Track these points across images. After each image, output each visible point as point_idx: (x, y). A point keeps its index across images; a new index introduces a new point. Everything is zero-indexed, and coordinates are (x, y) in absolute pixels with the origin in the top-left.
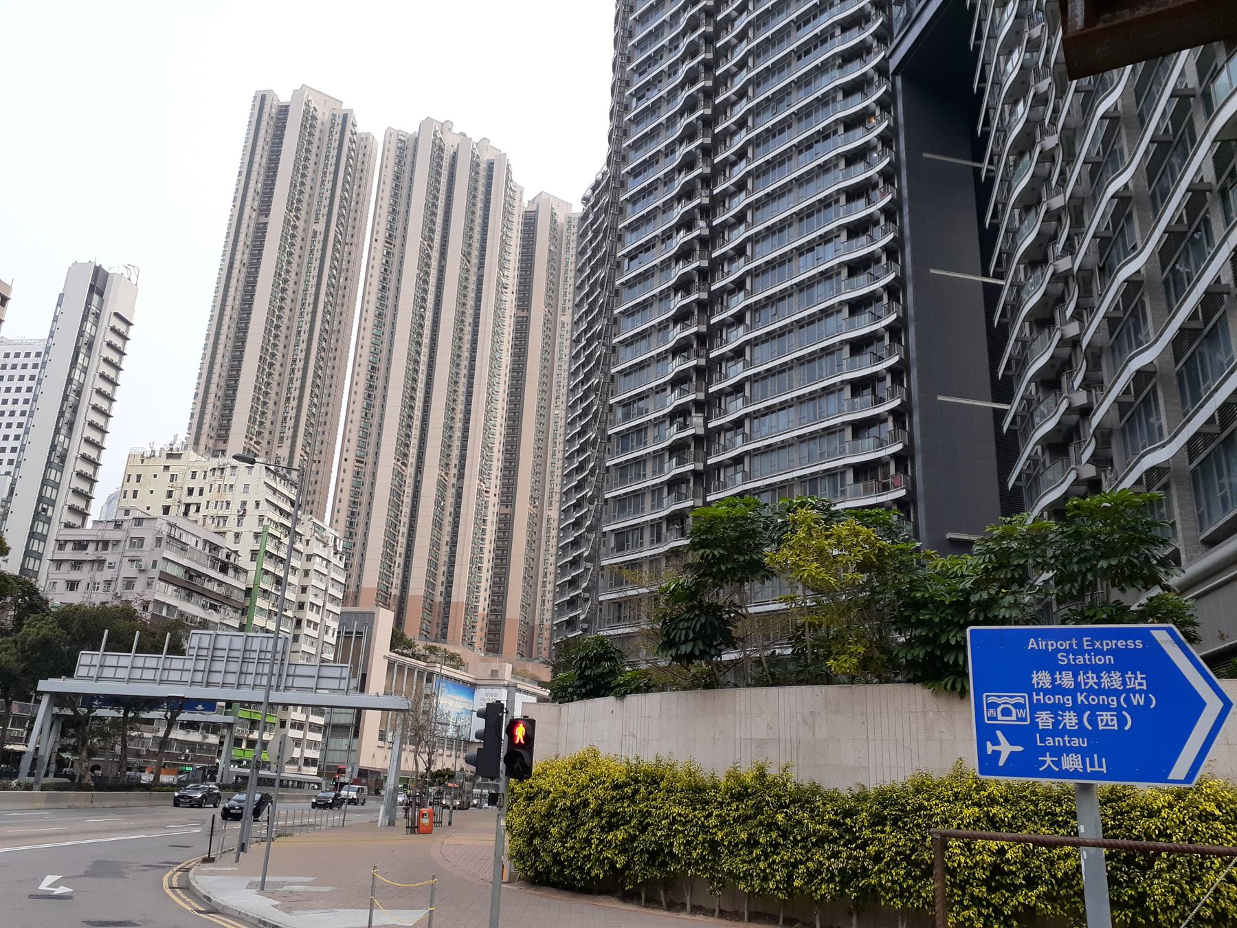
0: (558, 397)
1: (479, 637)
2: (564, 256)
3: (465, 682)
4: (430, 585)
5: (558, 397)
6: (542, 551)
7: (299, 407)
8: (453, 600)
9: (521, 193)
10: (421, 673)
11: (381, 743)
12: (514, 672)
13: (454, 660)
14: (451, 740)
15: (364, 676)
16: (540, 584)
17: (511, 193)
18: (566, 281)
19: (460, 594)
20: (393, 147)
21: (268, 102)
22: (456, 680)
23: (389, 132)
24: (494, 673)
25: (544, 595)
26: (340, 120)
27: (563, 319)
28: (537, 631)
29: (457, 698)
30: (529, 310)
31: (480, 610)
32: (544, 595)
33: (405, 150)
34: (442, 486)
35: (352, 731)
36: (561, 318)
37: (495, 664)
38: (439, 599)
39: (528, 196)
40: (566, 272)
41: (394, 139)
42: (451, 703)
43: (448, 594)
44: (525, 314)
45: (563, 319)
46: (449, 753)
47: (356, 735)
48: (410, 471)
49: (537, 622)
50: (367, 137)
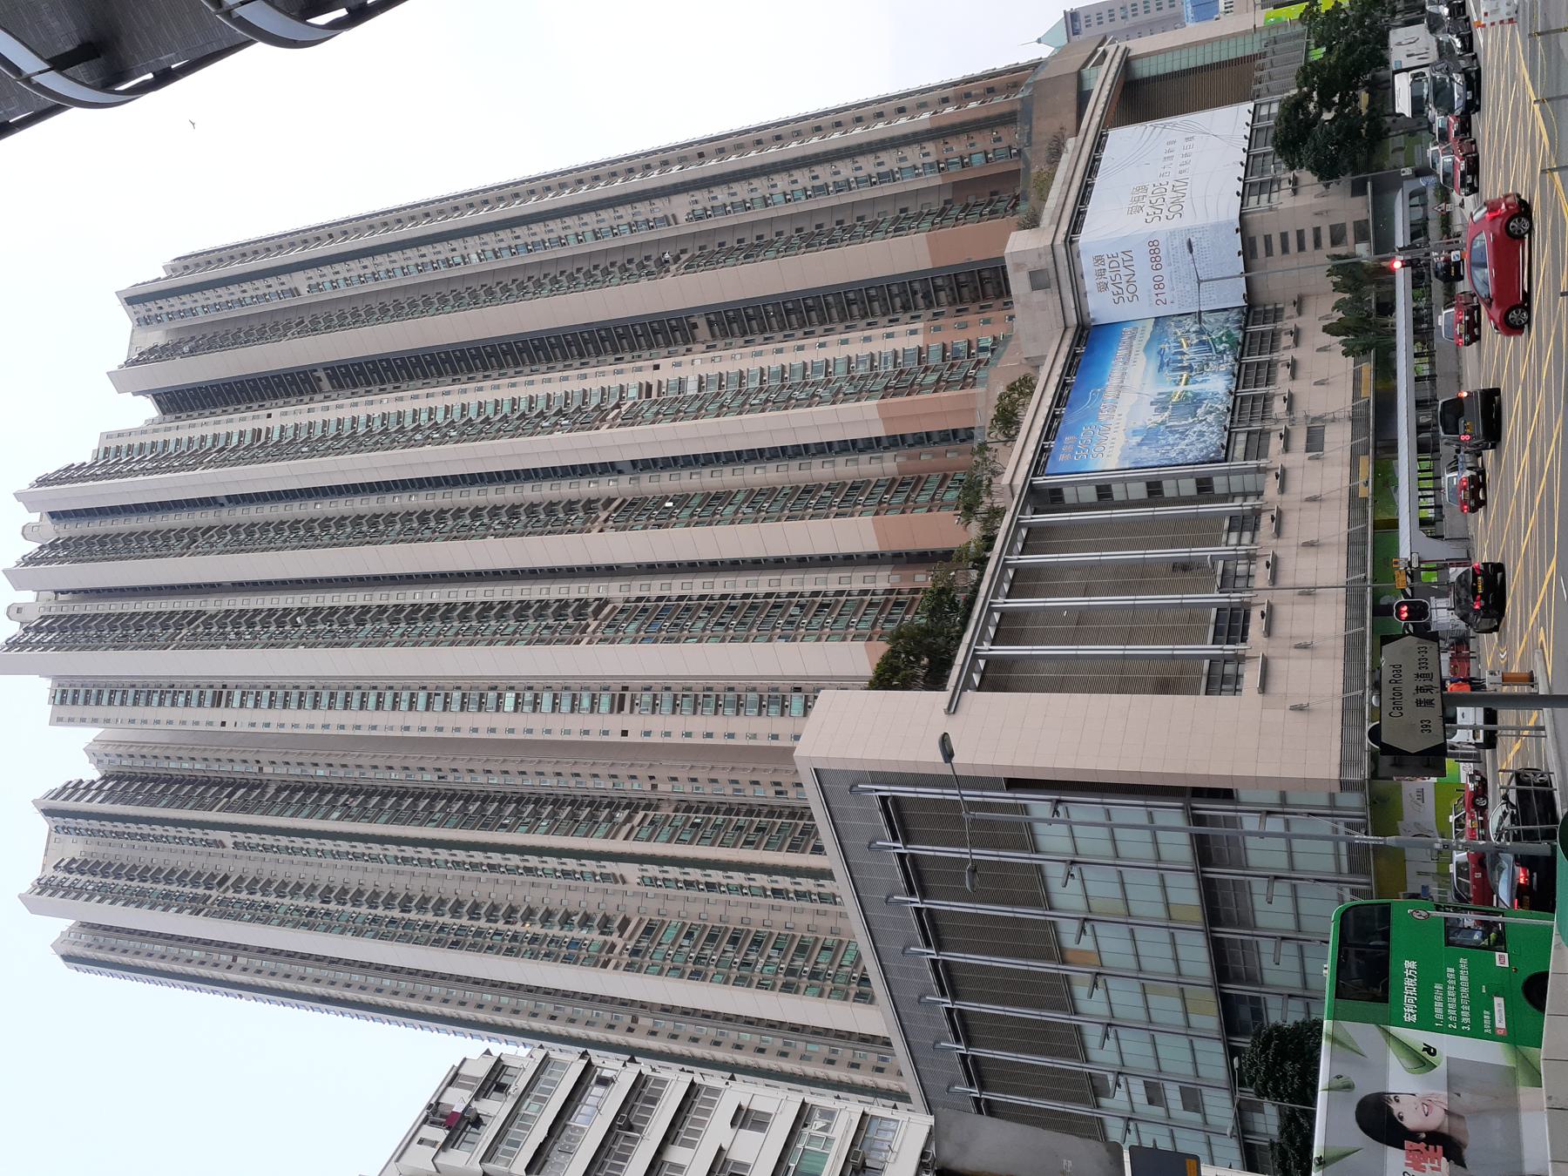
0: (448, 263)
1: (977, 329)
2: (202, 318)
3: (1071, 366)
4: (848, 497)
5: (448, 263)
6: (770, 213)
7: (540, 852)
8: (879, 431)
9: (109, 436)
10: (1036, 539)
11: (1251, 675)
12: (1033, 222)
13: (1007, 419)
14: (1242, 375)
15: (1013, 784)
16: (846, 198)
17: (117, 457)
18: (241, 302)
19: (862, 417)
20: (79, 711)
21: (78, 951)
22: (1060, 399)
23: (58, 720)
24: (1038, 280)
25: (869, 181)
26: (60, 821)
27: (304, 290)
28: (956, 173)
29: (1112, 382)
30: (313, 369)
31: (917, 341)
32: (869, 181)
33: (73, 697)
34: (632, 512)
35: (1207, 808)
36: (306, 297)
37: (1018, 284)
38: (888, 465)
39: (147, 410)
40: (229, 305)
41: (66, 711)
42: (1127, 400)
43: (871, 445)
44: (321, 374)
45: (304, 290)
46: (1283, 373)
47: (1226, 795)
48: (614, 590)
49: (935, 180)
50: (95, 753)
